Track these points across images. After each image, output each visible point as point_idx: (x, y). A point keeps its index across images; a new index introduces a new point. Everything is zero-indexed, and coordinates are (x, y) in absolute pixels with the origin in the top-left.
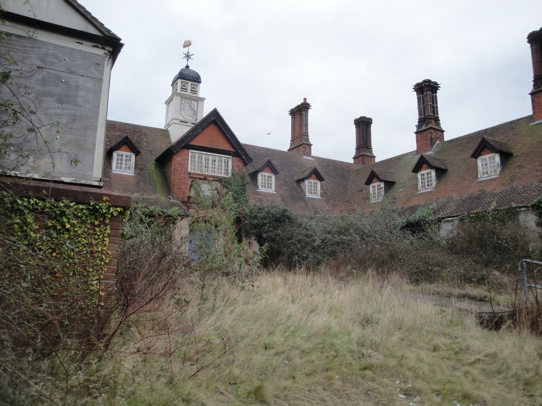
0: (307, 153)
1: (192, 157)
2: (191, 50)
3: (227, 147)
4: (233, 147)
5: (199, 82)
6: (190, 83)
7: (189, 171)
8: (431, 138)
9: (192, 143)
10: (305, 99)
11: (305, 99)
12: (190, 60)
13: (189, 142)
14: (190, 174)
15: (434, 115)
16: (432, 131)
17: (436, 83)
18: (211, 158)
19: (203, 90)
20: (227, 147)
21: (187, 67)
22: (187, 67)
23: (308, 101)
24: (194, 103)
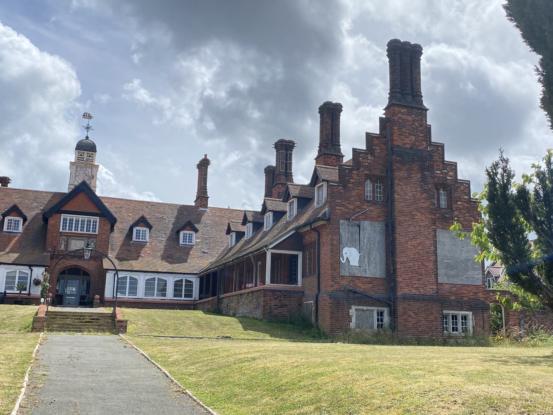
0: (204, 205)
1: (64, 219)
2: (91, 122)
3: (96, 211)
4: (100, 210)
5: (96, 151)
6: (86, 152)
7: (61, 230)
8: (279, 193)
9: (63, 209)
10: (206, 155)
11: (206, 155)
12: (90, 131)
13: (60, 208)
14: (61, 233)
15: (286, 170)
16: (280, 186)
17: (290, 142)
18: (80, 219)
19: (98, 158)
20: (96, 211)
21: (87, 138)
22: (87, 138)
23: (208, 158)
24: (90, 170)
